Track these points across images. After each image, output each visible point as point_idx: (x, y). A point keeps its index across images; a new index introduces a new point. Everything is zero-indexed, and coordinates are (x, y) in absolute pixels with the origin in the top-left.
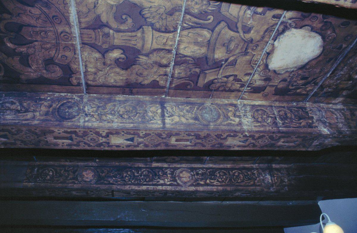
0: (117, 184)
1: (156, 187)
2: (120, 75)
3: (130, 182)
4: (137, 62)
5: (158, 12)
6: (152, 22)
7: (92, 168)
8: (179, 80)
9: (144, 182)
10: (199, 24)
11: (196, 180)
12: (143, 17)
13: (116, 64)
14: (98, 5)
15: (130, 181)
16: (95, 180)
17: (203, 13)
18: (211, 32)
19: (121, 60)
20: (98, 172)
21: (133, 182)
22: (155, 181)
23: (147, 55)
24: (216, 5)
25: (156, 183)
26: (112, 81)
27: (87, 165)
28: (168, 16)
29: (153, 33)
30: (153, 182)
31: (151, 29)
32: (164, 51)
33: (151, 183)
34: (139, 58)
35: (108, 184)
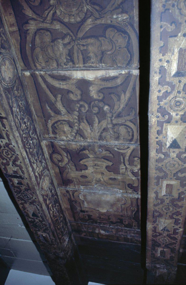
0: (15, 118)
1: (30, 166)
3: (22, 133)
7: (16, 70)
9: (28, 148)
11: (47, 196)
15: (23, 131)
16: (7, 85)
20: (15, 82)
21: (24, 135)
22: (33, 159)
25: (32, 161)
27: (15, 61)
30: (32, 158)
33: (30, 156)
35: (10, 106)
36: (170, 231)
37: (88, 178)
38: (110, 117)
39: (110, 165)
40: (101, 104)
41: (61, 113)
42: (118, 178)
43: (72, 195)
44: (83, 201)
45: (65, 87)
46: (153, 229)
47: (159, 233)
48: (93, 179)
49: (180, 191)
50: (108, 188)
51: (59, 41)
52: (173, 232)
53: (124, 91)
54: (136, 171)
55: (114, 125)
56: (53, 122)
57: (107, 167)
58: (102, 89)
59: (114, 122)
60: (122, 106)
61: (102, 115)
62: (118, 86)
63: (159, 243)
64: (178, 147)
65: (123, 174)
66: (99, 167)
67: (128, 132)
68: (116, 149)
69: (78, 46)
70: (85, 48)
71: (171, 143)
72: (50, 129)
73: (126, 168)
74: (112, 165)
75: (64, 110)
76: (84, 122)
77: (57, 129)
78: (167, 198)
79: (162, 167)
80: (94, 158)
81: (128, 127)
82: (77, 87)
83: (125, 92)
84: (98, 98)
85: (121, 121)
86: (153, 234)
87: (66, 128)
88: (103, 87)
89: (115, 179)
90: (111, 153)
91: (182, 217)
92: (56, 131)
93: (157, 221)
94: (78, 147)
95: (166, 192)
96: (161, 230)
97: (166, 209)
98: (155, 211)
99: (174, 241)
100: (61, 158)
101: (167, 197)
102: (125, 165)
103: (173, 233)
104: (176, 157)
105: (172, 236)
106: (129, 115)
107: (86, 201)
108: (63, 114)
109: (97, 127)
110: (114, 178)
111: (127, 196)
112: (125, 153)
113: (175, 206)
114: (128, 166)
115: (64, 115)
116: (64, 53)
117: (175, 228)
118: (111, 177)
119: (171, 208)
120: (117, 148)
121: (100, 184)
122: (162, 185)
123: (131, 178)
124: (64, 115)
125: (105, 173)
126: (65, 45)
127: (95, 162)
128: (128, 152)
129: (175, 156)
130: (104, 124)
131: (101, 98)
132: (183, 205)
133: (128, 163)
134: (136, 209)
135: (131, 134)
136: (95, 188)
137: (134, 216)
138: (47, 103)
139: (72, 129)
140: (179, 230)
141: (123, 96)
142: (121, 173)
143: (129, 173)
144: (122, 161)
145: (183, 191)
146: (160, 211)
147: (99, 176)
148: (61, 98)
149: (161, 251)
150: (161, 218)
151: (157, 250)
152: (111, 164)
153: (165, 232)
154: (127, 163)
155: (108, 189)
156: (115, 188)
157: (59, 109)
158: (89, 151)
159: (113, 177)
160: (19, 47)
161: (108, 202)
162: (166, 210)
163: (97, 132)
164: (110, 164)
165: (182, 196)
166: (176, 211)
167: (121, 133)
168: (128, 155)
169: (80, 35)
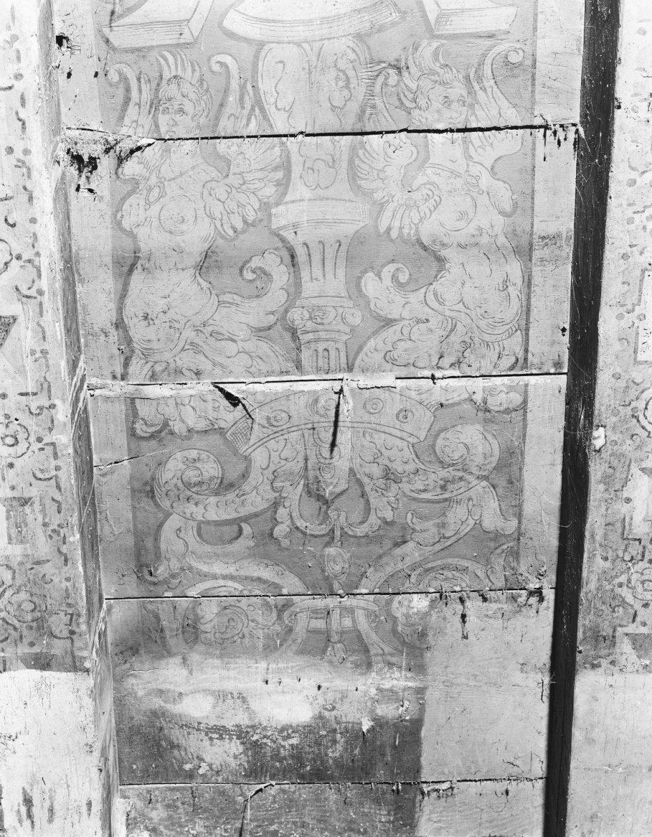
4: (406, 231)
5: (223, 197)
6: (257, 207)
10: (243, 87)
12: (244, 232)
13: (423, 290)
14: (224, 332)
17: (205, 86)
18: (266, 48)
19: (403, 278)
23: (382, 206)
24: (176, 60)
28: (233, 169)
29: (293, 202)
31: (281, 208)
32: (357, 162)
34: (389, 230)
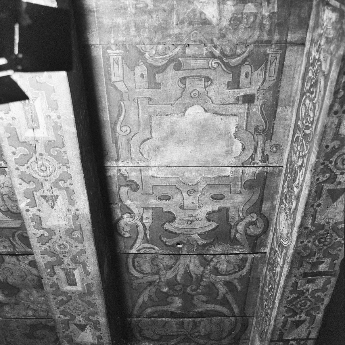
2: (31, 293)
8: (17, 246)
26: (43, 298)
36: (42, 196)
37: (211, 195)
38: (162, 282)
39: (167, 223)
40: (171, 292)
41: (223, 283)
42: (155, 201)
43: (259, 150)
44: (236, 138)
45: (209, 306)
46: (73, 198)
47: (60, 188)
48: (202, 194)
49: (55, 278)
50: (175, 176)
51: (203, 334)
52: (36, 197)
53: (145, 303)
54: (125, 216)
55: (157, 273)
56: (240, 273)
57: (173, 220)
58: (168, 304)
59: (157, 277)
60: (147, 292)
61: (172, 284)
62: (150, 307)
63: (51, 155)
64: (77, 325)
65: (147, 208)
66: (186, 218)
67: (139, 266)
68: (156, 248)
69: (186, 331)
70: (179, 330)
71: (86, 329)
72: (248, 265)
73: (141, 219)
74: (164, 224)
75: (219, 285)
76: (196, 275)
77: (238, 265)
78: (69, 265)
79: (88, 307)
80: (192, 234)
81: (140, 271)
82: (196, 305)
83: (144, 302)
84: (174, 298)
85: (150, 278)
86: (71, 184)
87: (223, 267)
88: (166, 306)
89: (161, 198)
90: (165, 243)
91: (34, 234)
92: (241, 262)
93: (71, 219)
94: (213, 248)
95: (74, 275)
96: (58, 196)
97: (65, 247)
98: (81, 240)
99: (23, 169)
100: (249, 229)
101: (70, 267)
102: (144, 225)
103: (33, 194)
104: (75, 316)
105: (32, 186)
106: (139, 284)
107: (231, 138)
108: (221, 282)
109: (180, 270)
110: (161, 200)
111: (140, 163)
112: (143, 243)
113: (53, 253)
114: (139, 223)
115: (221, 281)
116: (201, 327)
117: (36, 208)
118: (167, 202)
119: (57, 249)
120: (154, 249)
121: (189, 184)
122: (83, 284)
123: (132, 203)
124: (221, 281)
125: (178, 208)
126: (199, 332)
127: (191, 227)
128: (139, 245)
129: (77, 318)
130: (170, 275)
131: (170, 297)
132: (42, 256)
133: (138, 228)
134: (118, 129)
135: (136, 264)
136: (201, 175)
137: (122, 103)
138: (237, 291)
139: (216, 266)
140: (28, 204)
141: (146, 299)
142: (151, 211)
143: (136, 211)
144: (148, 232)
145: (52, 278)
146: (72, 242)
147: (189, 201)
148: (217, 297)
149: (38, 127)
150: (68, 227)
151: (48, 129)
152: (166, 225)
153: (48, 194)
154: (141, 228)
155: (175, 174)
156: (161, 179)
157: (225, 287)
158: (198, 244)
159: (164, 202)
160: (246, 331)
161: (179, 142)
162: (63, 244)
163: (181, 265)
164: (167, 226)
165: (49, 270)
166: (48, 244)
167: (148, 264)
168: (139, 241)
169: (183, 337)
